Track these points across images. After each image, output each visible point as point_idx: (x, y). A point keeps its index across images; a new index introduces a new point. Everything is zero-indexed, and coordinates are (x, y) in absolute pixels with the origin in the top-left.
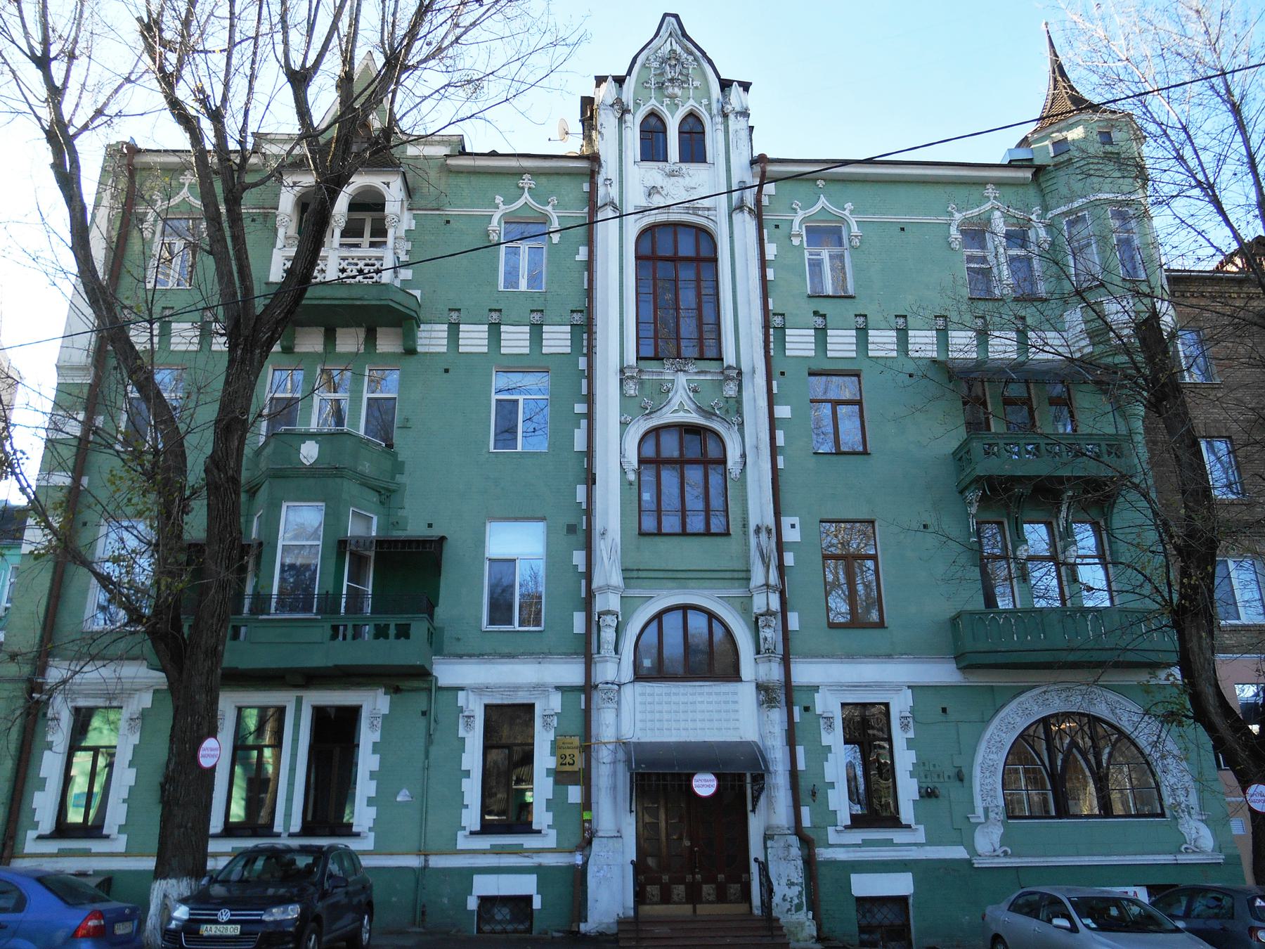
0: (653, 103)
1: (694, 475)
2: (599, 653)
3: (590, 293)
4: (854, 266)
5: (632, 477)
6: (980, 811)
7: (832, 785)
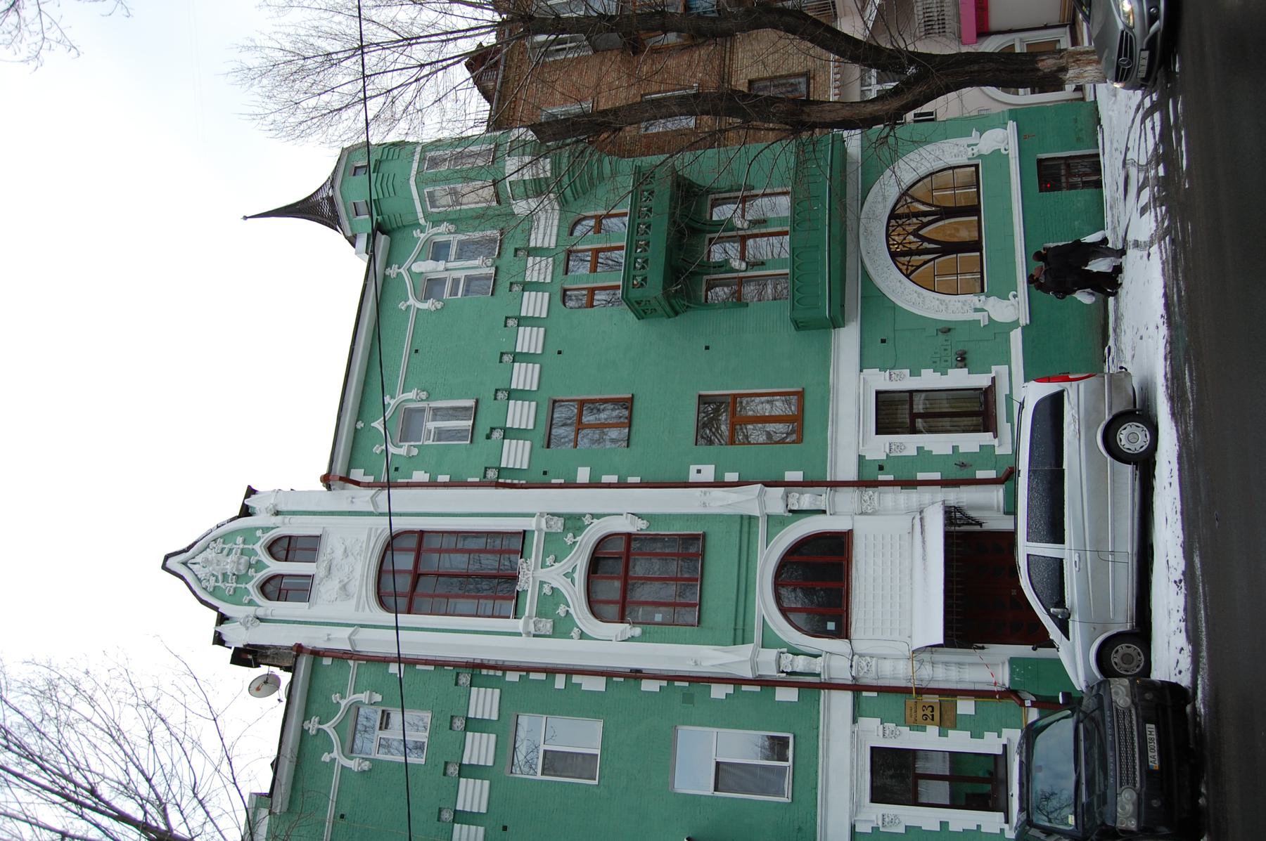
0: (252, 587)
1: (640, 568)
2: (819, 675)
3: (439, 664)
4: (446, 398)
5: (637, 631)
6: (978, 316)
7: (955, 448)
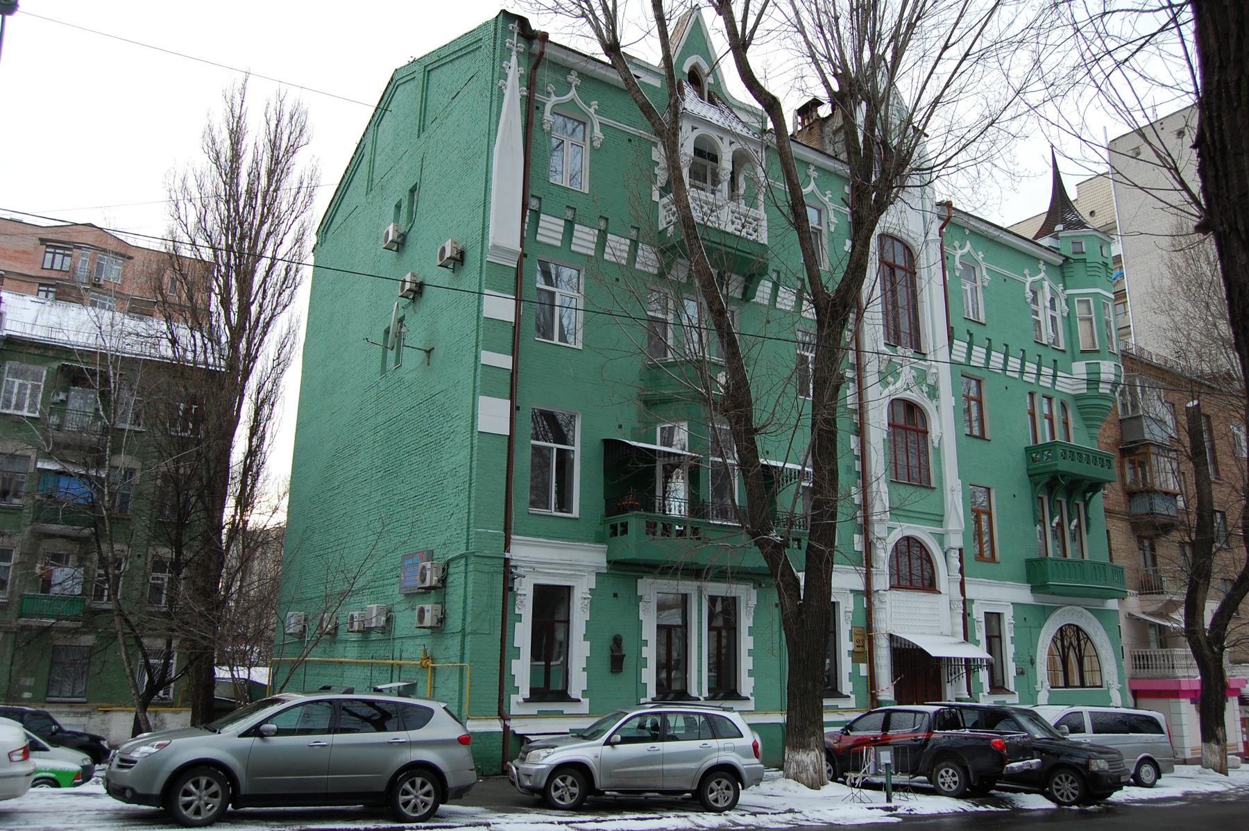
1: (912, 437)
